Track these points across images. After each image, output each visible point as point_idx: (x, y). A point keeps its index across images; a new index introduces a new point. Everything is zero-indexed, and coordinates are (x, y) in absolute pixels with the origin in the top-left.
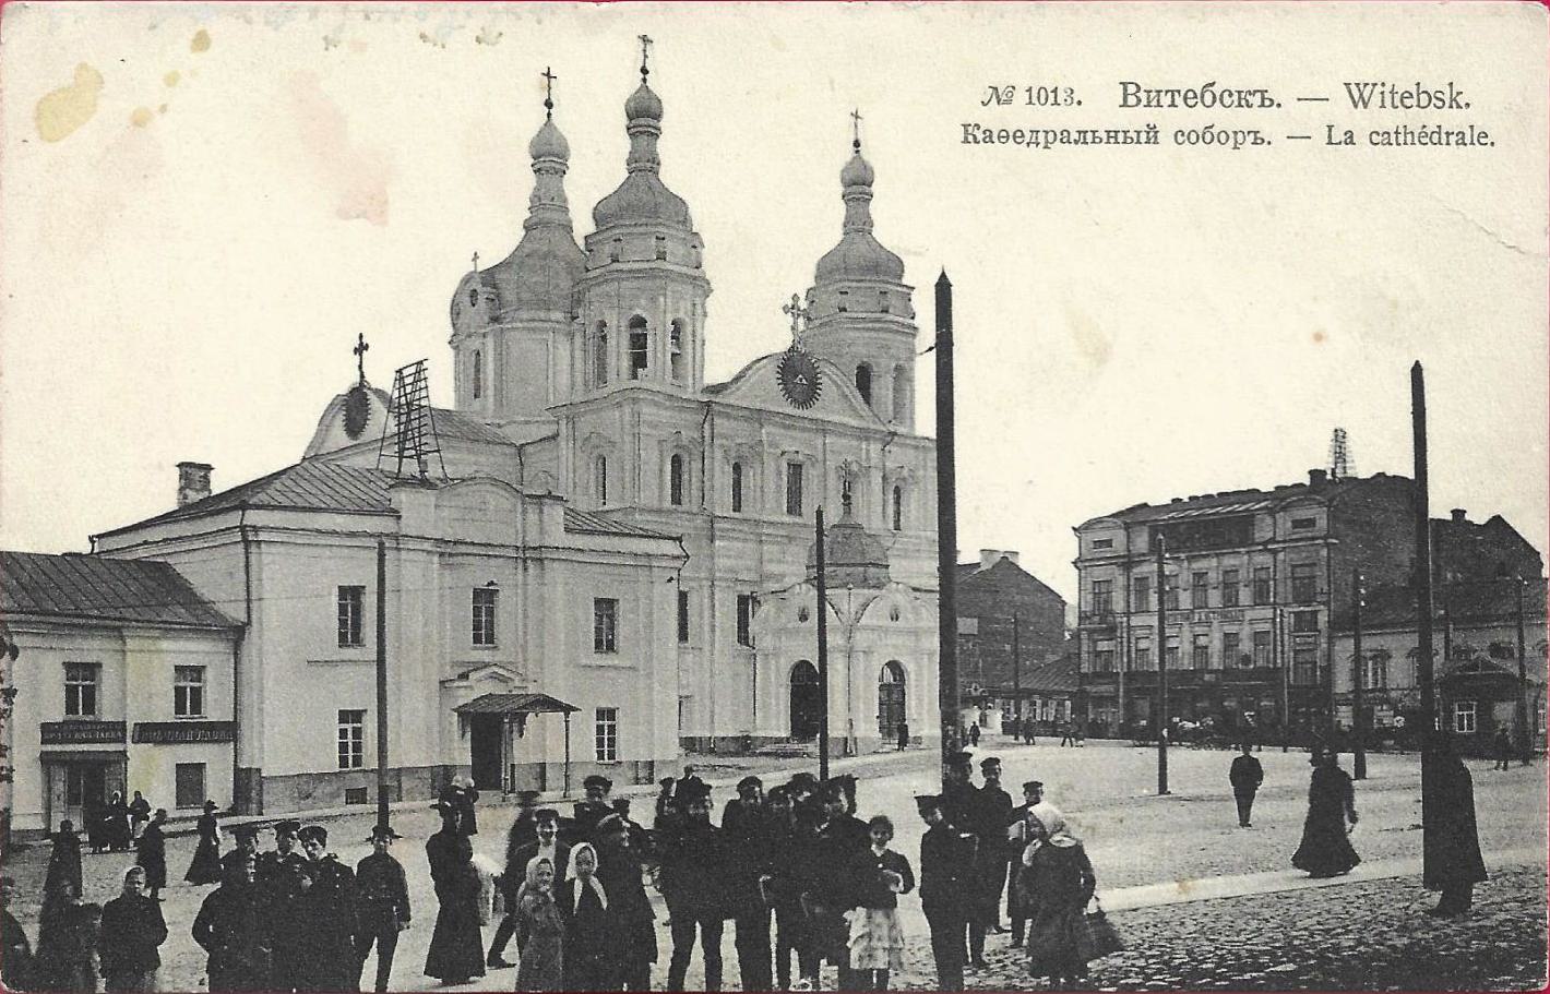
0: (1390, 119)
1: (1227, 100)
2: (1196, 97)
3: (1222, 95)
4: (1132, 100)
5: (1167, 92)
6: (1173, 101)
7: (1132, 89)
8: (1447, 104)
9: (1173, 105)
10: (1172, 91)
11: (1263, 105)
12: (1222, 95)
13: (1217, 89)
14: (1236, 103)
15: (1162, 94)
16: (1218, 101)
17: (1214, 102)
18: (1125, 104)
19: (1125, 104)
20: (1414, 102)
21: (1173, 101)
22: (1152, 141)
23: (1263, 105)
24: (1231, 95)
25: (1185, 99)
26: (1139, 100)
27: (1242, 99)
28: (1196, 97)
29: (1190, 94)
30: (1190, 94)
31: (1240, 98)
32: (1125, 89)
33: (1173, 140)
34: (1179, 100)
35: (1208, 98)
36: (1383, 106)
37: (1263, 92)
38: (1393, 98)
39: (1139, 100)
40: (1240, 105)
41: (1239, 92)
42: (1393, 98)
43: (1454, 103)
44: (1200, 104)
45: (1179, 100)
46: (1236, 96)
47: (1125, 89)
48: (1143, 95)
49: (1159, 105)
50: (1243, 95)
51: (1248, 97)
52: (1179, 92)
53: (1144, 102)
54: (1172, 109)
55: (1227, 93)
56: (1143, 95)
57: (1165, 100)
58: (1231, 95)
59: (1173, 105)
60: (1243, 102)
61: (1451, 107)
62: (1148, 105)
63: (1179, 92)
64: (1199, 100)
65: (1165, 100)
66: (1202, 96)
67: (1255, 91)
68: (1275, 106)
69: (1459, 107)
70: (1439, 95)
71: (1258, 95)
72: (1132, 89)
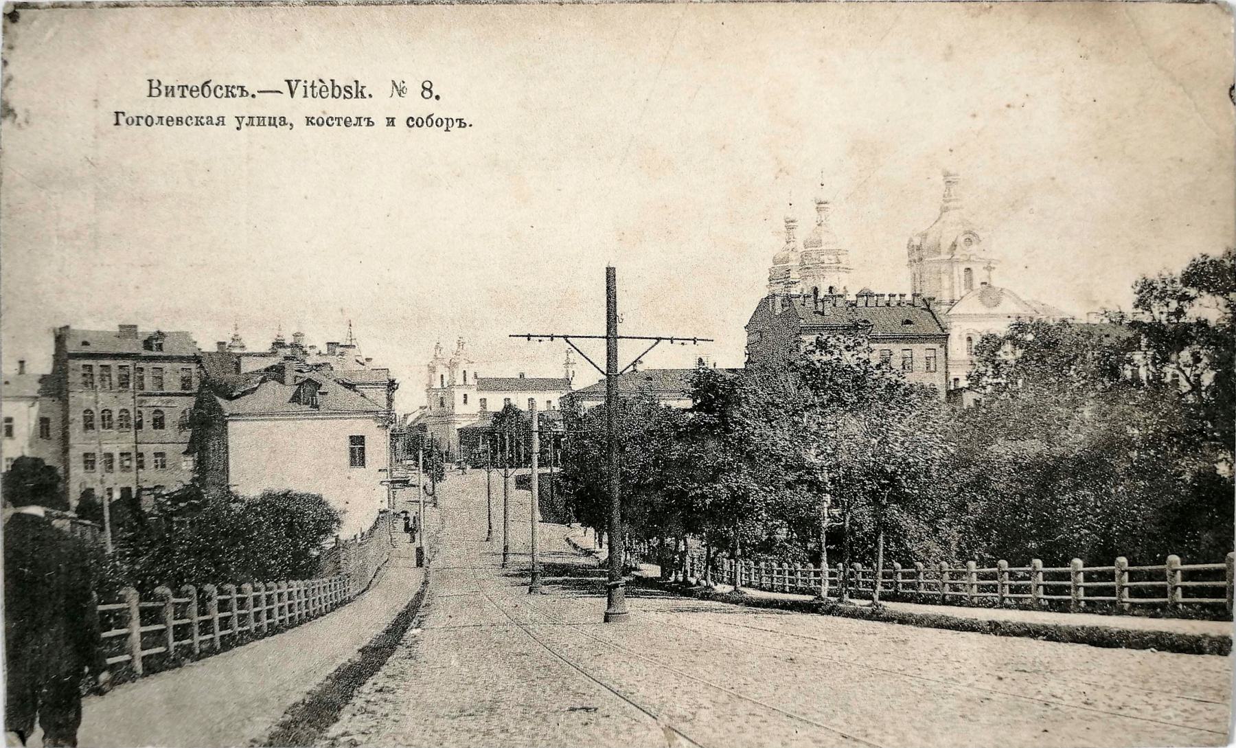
0: (316, 107)
1: (219, 93)
4: (155, 92)
5: (179, 86)
6: (183, 91)
7: (155, 84)
8: (354, 95)
9: (183, 96)
11: (242, 95)
13: (212, 85)
14: (225, 95)
15: (176, 88)
18: (150, 95)
19: (150, 95)
20: (330, 92)
21: (183, 91)
23: (242, 95)
24: (221, 89)
25: (191, 91)
26: (160, 92)
28: (198, 90)
29: (195, 89)
32: (151, 85)
34: (187, 93)
35: (206, 89)
36: (305, 96)
37: (242, 87)
38: (313, 91)
40: (227, 96)
42: (313, 91)
43: (360, 94)
44: (201, 95)
45: (187, 93)
46: (225, 89)
47: (151, 85)
48: (162, 88)
49: (173, 96)
50: (230, 89)
51: (235, 91)
52: (187, 86)
53: (164, 92)
55: (218, 88)
56: (162, 88)
57: (178, 93)
58: (221, 89)
59: (183, 96)
60: (230, 94)
61: (357, 96)
63: (187, 86)
64: (200, 92)
65: (178, 93)
68: (250, 96)
69: (363, 96)
70: (348, 89)
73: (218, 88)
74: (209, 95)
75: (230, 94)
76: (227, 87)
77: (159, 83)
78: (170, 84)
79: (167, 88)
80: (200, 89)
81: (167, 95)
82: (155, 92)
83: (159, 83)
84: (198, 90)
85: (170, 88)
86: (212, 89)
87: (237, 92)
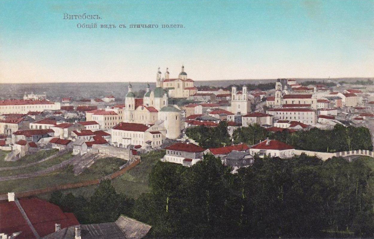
6: (76, 16)
9: (76, 19)
10: (76, 16)
11: (97, 19)
14: (91, 18)
15: (73, 16)
16: (86, 17)
17: (86, 18)
21: (76, 16)
22: (106, 27)
26: (68, 18)
27: (92, 17)
29: (80, 16)
33: (77, 27)
37: (97, 15)
39: (68, 18)
40: (92, 19)
45: (77, 17)
46: (91, 16)
50: (93, 16)
53: (69, 18)
56: (69, 16)
57: (74, 17)
58: (90, 16)
59: (76, 19)
60: (93, 18)
65: (74, 17)
67: (96, 15)
68: (100, 19)
71: (96, 16)
72: (66, 15)
74: (86, 18)
75: (93, 18)
76: (92, 16)
82: (66, 17)
86: (87, 16)
87: (96, 17)
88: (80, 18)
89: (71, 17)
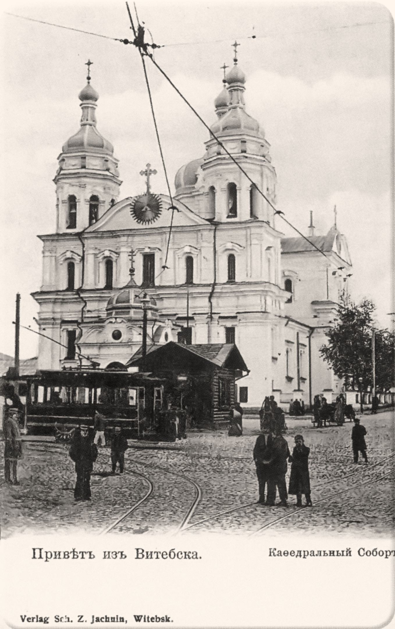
1: (180, 556)
2: (167, 554)
3: (178, 554)
4: (140, 556)
5: (155, 552)
6: (157, 556)
7: (140, 551)
9: (157, 558)
12: (178, 554)
14: (184, 557)
15: (153, 553)
18: (137, 558)
19: (137, 558)
21: (157, 556)
24: (181, 554)
25: (162, 555)
30: (164, 553)
31: (185, 555)
35: (172, 554)
39: (143, 556)
40: (185, 558)
41: (185, 553)
44: (169, 557)
46: (184, 554)
49: (151, 558)
50: (187, 554)
51: (190, 555)
52: (160, 552)
53: (145, 557)
54: (157, 559)
55: (180, 553)
56: (145, 554)
57: (154, 556)
58: (181, 554)
59: (157, 558)
60: (187, 557)
62: (147, 558)
64: (168, 556)
65: (154, 556)
66: (170, 555)
73: (180, 553)
74: (174, 558)
75: (187, 557)
76: (185, 553)
77: (143, 551)
78: (149, 551)
79: (147, 553)
80: (168, 553)
81: (147, 558)
82: (140, 556)
83: (143, 551)
84: (167, 554)
85: (149, 553)
86: (176, 553)
88: (165, 556)
89: (149, 555)
